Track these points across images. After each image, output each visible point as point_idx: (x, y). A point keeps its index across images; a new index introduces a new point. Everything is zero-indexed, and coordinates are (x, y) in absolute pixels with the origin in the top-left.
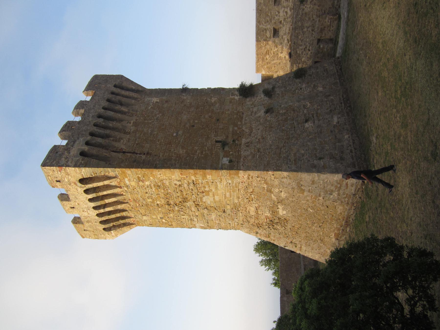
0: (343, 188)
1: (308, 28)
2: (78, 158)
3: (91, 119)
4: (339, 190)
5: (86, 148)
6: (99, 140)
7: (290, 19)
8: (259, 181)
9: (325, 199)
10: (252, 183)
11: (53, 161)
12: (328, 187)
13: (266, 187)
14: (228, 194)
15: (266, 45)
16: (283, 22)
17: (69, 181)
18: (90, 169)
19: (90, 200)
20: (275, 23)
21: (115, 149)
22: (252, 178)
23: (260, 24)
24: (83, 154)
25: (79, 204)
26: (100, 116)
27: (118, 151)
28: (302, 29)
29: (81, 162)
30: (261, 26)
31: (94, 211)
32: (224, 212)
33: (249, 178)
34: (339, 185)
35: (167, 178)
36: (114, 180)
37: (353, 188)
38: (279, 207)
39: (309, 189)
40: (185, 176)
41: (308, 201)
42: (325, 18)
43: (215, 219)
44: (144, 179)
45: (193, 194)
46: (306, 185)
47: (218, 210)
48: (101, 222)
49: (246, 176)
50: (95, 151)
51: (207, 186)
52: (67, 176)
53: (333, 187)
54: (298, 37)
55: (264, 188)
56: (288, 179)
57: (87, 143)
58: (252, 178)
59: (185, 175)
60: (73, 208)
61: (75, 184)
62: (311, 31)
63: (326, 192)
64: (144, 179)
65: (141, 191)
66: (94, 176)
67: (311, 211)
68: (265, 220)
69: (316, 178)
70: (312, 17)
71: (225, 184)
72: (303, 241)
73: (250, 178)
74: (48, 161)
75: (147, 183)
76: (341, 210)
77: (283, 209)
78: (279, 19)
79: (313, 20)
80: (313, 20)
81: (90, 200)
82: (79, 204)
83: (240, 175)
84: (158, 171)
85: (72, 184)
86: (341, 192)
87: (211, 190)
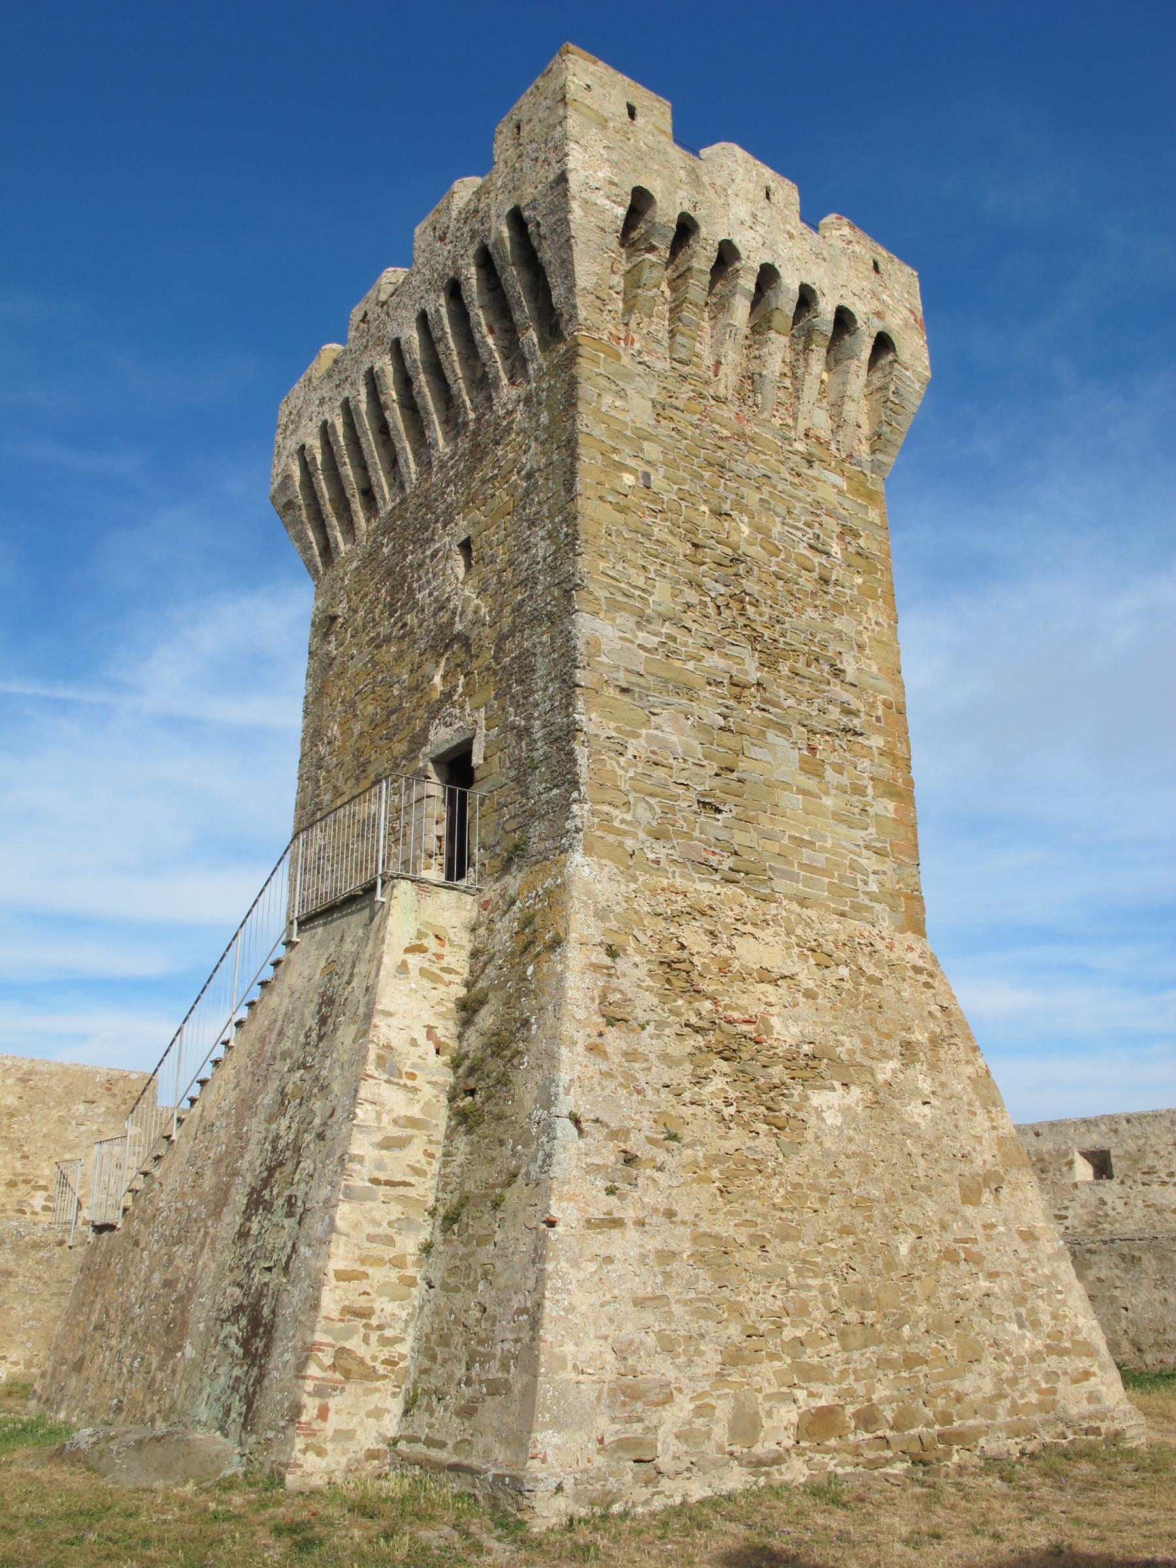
8: (930, 1012)
9: (986, 1300)
25: (791, 237)
33: (918, 970)
34: (1068, 1345)
38: (856, 1092)
41: (944, 1227)
43: (665, 745)
51: (845, 780)
58: (927, 985)
67: (904, 1250)
71: (863, 861)
75: (836, 548)
83: (910, 935)
86: (1052, 1362)
87: (827, 793)
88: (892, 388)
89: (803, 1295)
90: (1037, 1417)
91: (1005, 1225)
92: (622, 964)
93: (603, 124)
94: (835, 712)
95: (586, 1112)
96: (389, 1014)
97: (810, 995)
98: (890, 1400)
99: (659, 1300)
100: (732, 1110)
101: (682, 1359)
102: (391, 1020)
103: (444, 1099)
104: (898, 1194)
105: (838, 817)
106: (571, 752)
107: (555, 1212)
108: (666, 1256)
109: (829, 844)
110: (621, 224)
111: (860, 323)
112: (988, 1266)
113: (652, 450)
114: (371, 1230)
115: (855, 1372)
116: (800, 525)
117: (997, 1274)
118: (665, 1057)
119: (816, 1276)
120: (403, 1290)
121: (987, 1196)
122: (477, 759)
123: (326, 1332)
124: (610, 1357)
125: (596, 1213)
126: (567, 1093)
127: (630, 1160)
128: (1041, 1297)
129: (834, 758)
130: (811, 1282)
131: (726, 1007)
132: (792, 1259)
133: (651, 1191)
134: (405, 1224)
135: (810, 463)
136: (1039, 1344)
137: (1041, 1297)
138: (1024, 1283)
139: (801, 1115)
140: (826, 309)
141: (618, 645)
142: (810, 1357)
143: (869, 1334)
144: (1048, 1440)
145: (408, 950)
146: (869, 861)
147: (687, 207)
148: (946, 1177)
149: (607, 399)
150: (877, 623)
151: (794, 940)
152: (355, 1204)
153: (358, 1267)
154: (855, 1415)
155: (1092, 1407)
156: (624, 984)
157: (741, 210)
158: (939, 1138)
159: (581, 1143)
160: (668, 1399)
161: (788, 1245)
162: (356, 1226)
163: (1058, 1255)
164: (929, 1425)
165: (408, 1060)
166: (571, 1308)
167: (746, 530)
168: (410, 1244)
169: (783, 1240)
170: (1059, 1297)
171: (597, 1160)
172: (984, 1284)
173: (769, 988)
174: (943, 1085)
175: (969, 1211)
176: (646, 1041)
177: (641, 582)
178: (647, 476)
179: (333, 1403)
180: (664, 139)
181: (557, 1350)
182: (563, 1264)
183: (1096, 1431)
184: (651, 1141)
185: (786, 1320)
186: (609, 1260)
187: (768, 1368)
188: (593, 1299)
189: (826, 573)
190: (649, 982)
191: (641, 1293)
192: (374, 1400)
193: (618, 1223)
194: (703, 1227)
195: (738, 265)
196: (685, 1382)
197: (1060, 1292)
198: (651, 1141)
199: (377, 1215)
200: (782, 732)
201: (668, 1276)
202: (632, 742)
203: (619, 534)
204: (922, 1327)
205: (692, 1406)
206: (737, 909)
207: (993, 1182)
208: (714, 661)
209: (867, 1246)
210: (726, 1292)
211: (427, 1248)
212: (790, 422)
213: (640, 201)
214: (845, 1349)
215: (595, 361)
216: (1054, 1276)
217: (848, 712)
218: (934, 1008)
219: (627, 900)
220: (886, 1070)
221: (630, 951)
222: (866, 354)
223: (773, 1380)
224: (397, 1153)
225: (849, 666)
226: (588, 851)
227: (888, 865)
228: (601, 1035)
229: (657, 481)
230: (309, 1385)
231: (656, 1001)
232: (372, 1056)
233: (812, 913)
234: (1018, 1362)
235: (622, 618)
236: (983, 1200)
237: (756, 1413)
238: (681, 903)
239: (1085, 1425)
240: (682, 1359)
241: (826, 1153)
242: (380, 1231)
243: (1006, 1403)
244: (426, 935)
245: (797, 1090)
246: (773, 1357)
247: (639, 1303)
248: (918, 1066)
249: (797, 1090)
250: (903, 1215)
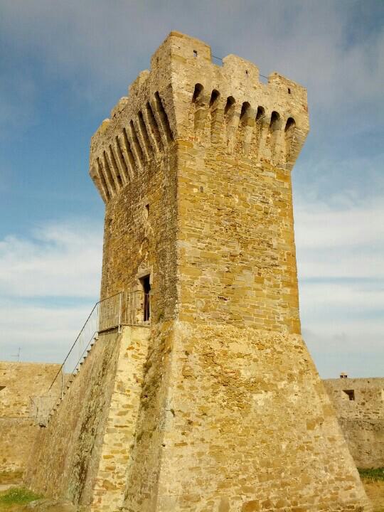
12: (334, 463)
25: (255, 88)
33: (296, 347)
37: (349, 499)
38: (270, 393)
39: (318, 437)
40: (286, 257)
43: (206, 281)
46: (323, 430)
51: (271, 283)
53: (338, 470)
58: (300, 352)
61: (289, 111)
67: (284, 447)
69: (339, 443)
71: (278, 311)
72: (206, 445)
75: (271, 201)
76: (308, 493)
77: (266, 401)
83: (295, 334)
86: (337, 483)
88: (294, 137)
89: (247, 464)
90: (329, 503)
92: (191, 357)
93: (184, 61)
94: (268, 260)
95: (175, 408)
96: (122, 371)
97: (255, 360)
98: (275, 498)
99: (198, 468)
100: (225, 403)
101: (204, 487)
102: (122, 373)
103: (139, 398)
104: (283, 427)
105: (269, 297)
106: (175, 287)
107: (165, 442)
108: (200, 454)
109: (265, 306)
110: (191, 99)
111: (281, 116)
112: (315, 451)
113: (203, 178)
114: (114, 442)
115: (263, 489)
116: (258, 194)
118: (203, 388)
119: (251, 457)
120: (125, 461)
121: (317, 426)
122: (151, 282)
123: (101, 475)
124: (181, 488)
125: (178, 441)
126: (170, 402)
127: (190, 423)
129: (268, 276)
130: (249, 460)
131: (225, 368)
132: (244, 452)
133: (196, 433)
134: (126, 439)
135: (263, 170)
136: (333, 478)
138: (329, 456)
139: (249, 403)
140: (268, 114)
141: (191, 249)
142: (248, 484)
143: (269, 476)
144: (333, 510)
145: (128, 349)
146: (279, 310)
147: (215, 87)
148: (302, 421)
149: (188, 162)
151: (251, 341)
152: (110, 434)
153: (111, 454)
154: (263, 503)
155: (351, 499)
156: (190, 364)
157: (236, 83)
158: (300, 407)
159: (174, 419)
160: (199, 500)
161: (242, 447)
162: (110, 441)
163: (343, 446)
164: (289, 506)
165: (128, 385)
166: (169, 472)
167: (237, 200)
168: (127, 446)
169: (241, 446)
170: (342, 460)
171: (179, 424)
172: (313, 457)
173: (241, 359)
174: (303, 388)
175: (310, 432)
176: (197, 383)
177: (199, 226)
178: (202, 188)
179: (102, 497)
180: (208, 62)
181: (164, 486)
182: (167, 459)
183: (353, 507)
184: (197, 416)
185: (240, 473)
186: (182, 456)
187: (233, 489)
189: (266, 210)
190: (199, 362)
191: (192, 466)
192: (115, 496)
193: (185, 444)
194: (213, 444)
195: (235, 104)
196: (205, 495)
198: (197, 416)
199: (117, 437)
201: (201, 460)
202: (196, 281)
203: (192, 210)
204: (289, 473)
205: (206, 502)
206: (231, 333)
207: (320, 421)
208: (225, 249)
209: (270, 446)
210: (220, 464)
211: (132, 447)
212: (255, 156)
213: (198, 88)
214: (260, 481)
215: (184, 149)
216: (341, 453)
217: (273, 259)
218: (302, 361)
219: (193, 335)
220: (281, 385)
221: (193, 352)
222: (284, 127)
223: (234, 492)
224: (123, 416)
225: (274, 243)
226: (181, 319)
227: (288, 310)
228: (182, 382)
229: (206, 188)
230: (95, 492)
231: (201, 368)
232: (116, 386)
233: (259, 331)
235: (192, 240)
236: (315, 428)
237: (228, 504)
238: (211, 334)
239: (348, 505)
240: (204, 487)
241: (258, 415)
242: (118, 442)
243: (319, 498)
244: (133, 343)
245: (249, 395)
246: (235, 485)
247: (191, 469)
249: (249, 395)
250: (285, 435)
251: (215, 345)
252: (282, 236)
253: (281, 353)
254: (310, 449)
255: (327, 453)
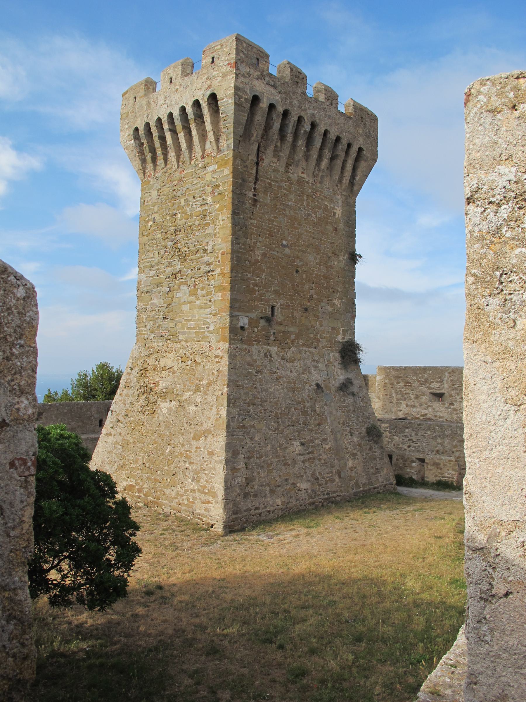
0: (203, 497)
1: (442, 444)
2: (248, 92)
3: (310, 111)
4: (199, 491)
5: (264, 105)
6: (277, 125)
7: (455, 418)
8: (213, 373)
9: (185, 470)
10: (209, 362)
11: (244, 54)
12: (204, 476)
13: (204, 382)
14: (192, 324)
15: (419, 381)
16: (452, 407)
17: (214, 77)
18: (233, 112)
19: (183, 109)
20: (451, 396)
21: (262, 149)
22: (218, 362)
23: (449, 373)
24: (256, 100)
26: (313, 125)
27: (260, 155)
28: (439, 436)
29: (242, 98)
30: (447, 374)
31: (166, 115)
32: (164, 318)
33: (217, 357)
34: (207, 491)
35: (217, 230)
36: (215, 148)
37: (202, 511)
38: (174, 403)
40: (220, 258)
41: (183, 445)
42: (453, 470)
43: (153, 304)
44: (216, 194)
45: (192, 270)
47: (167, 310)
48: (148, 125)
49: (220, 354)
50: (260, 117)
51: (204, 292)
52: (221, 75)
54: (429, 429)
55: (202, 380)
56: (216, 416)
57: (272, 107)
58: (218, 362)
59: (222, 258)
60: (171, 82)
61: (209, 87)
62: (437, 448)
63: (197, 472)
64: (216, 194)
65: (197, 189)
66: (221, 116)
67: (168, 451)
68: (152, 382)
69: (217, 459)
70: (457, 451)
71: (208, 320)
72: (121, 438)
73: (217, 360)
74: (245, 45)
75: (209, 199)
76: (170, 494)
78: (456, 401)
79: (453, 452)
80: (453, 452)
81: (183, 109)
82: (177, 90)
83: (221, 343)
84: (228, 217)
85: (208, 83)
86: (198, 494)
87: (198, 300)
91: (204, 448)
97: (174, 373)
112: (192, 461)
116: (198, 199)
117: (193, 463)
128: (205, 474)
137: (205, 474)
138: (201, 468)
150: (222, 220)
154: (137, 489)
163: (220, 462)
170: (212, 475)
172: (187, 465)
173: (164, 372)
174: (206, 399)
175: (194, 442)
177: (152, 256)
188: (102, 450)
189: (205, 213)
193: (111, 435)
194: (125, 438)
197: (214, 474)
200: (185, 284)
216: (214, 468)
234: (186, 491)
243: (177, 500)
248: (199, 393)
251: (151, 361)
252: (218, 235)
253: (200, 364)
254: (188, 457)
255: (201, 465)
